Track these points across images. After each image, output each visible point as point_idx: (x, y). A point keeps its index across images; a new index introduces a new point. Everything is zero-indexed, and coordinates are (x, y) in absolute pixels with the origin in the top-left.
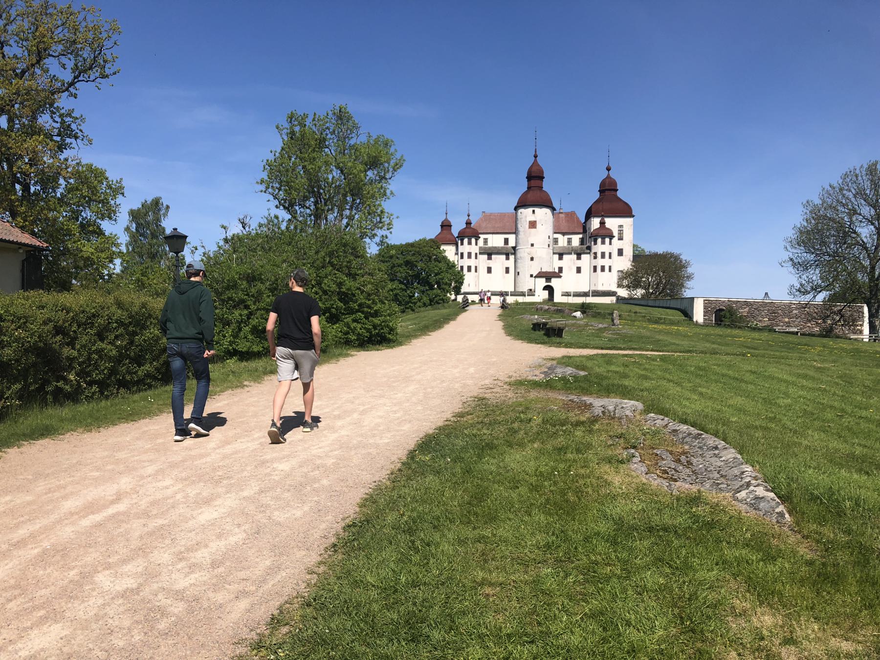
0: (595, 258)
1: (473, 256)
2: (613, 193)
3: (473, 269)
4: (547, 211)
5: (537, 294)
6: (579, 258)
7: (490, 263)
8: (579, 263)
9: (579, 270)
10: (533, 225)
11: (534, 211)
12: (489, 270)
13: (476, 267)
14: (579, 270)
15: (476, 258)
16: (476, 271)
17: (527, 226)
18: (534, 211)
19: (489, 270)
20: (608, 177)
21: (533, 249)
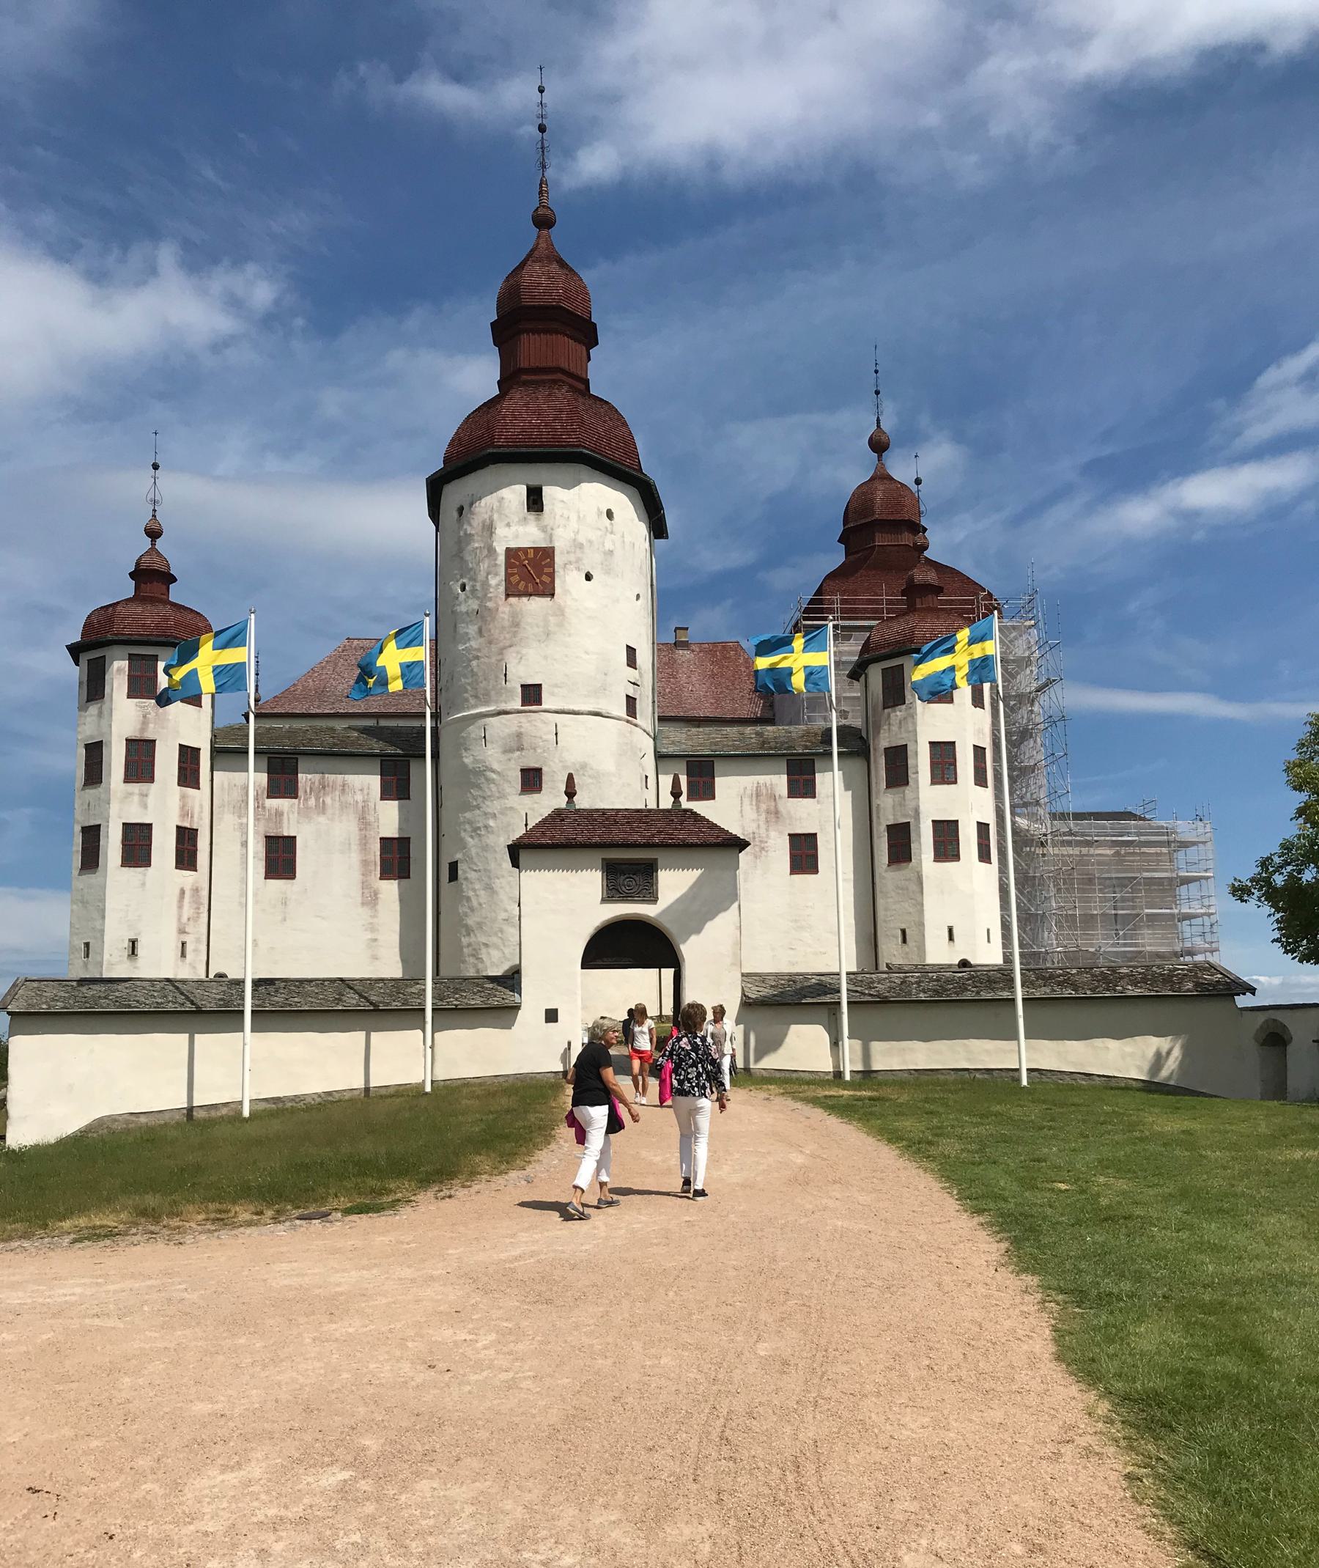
0: (899, 772)
1: (166, 763)
2: (906, 539)
3: (164, 846)
4: (621, 502)
5: (532, 1000)
6: (802, 786)
7: (290, 817)
8: (803, 814)
9: (804, 854)
10: (533, 572)
11: (535, 501)
12: (280, 858)
13: (186, 838)
14: (804, 854)
15: (188, 776)
16: (186, 858)
17: (497, 582)
18: (535, 501)
19: (280, 858)
20: (882, 476)
21: (537, 725)
